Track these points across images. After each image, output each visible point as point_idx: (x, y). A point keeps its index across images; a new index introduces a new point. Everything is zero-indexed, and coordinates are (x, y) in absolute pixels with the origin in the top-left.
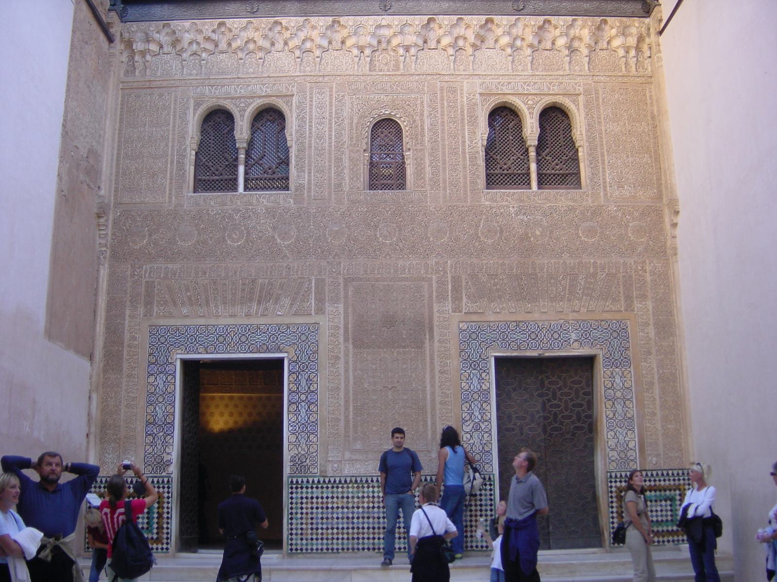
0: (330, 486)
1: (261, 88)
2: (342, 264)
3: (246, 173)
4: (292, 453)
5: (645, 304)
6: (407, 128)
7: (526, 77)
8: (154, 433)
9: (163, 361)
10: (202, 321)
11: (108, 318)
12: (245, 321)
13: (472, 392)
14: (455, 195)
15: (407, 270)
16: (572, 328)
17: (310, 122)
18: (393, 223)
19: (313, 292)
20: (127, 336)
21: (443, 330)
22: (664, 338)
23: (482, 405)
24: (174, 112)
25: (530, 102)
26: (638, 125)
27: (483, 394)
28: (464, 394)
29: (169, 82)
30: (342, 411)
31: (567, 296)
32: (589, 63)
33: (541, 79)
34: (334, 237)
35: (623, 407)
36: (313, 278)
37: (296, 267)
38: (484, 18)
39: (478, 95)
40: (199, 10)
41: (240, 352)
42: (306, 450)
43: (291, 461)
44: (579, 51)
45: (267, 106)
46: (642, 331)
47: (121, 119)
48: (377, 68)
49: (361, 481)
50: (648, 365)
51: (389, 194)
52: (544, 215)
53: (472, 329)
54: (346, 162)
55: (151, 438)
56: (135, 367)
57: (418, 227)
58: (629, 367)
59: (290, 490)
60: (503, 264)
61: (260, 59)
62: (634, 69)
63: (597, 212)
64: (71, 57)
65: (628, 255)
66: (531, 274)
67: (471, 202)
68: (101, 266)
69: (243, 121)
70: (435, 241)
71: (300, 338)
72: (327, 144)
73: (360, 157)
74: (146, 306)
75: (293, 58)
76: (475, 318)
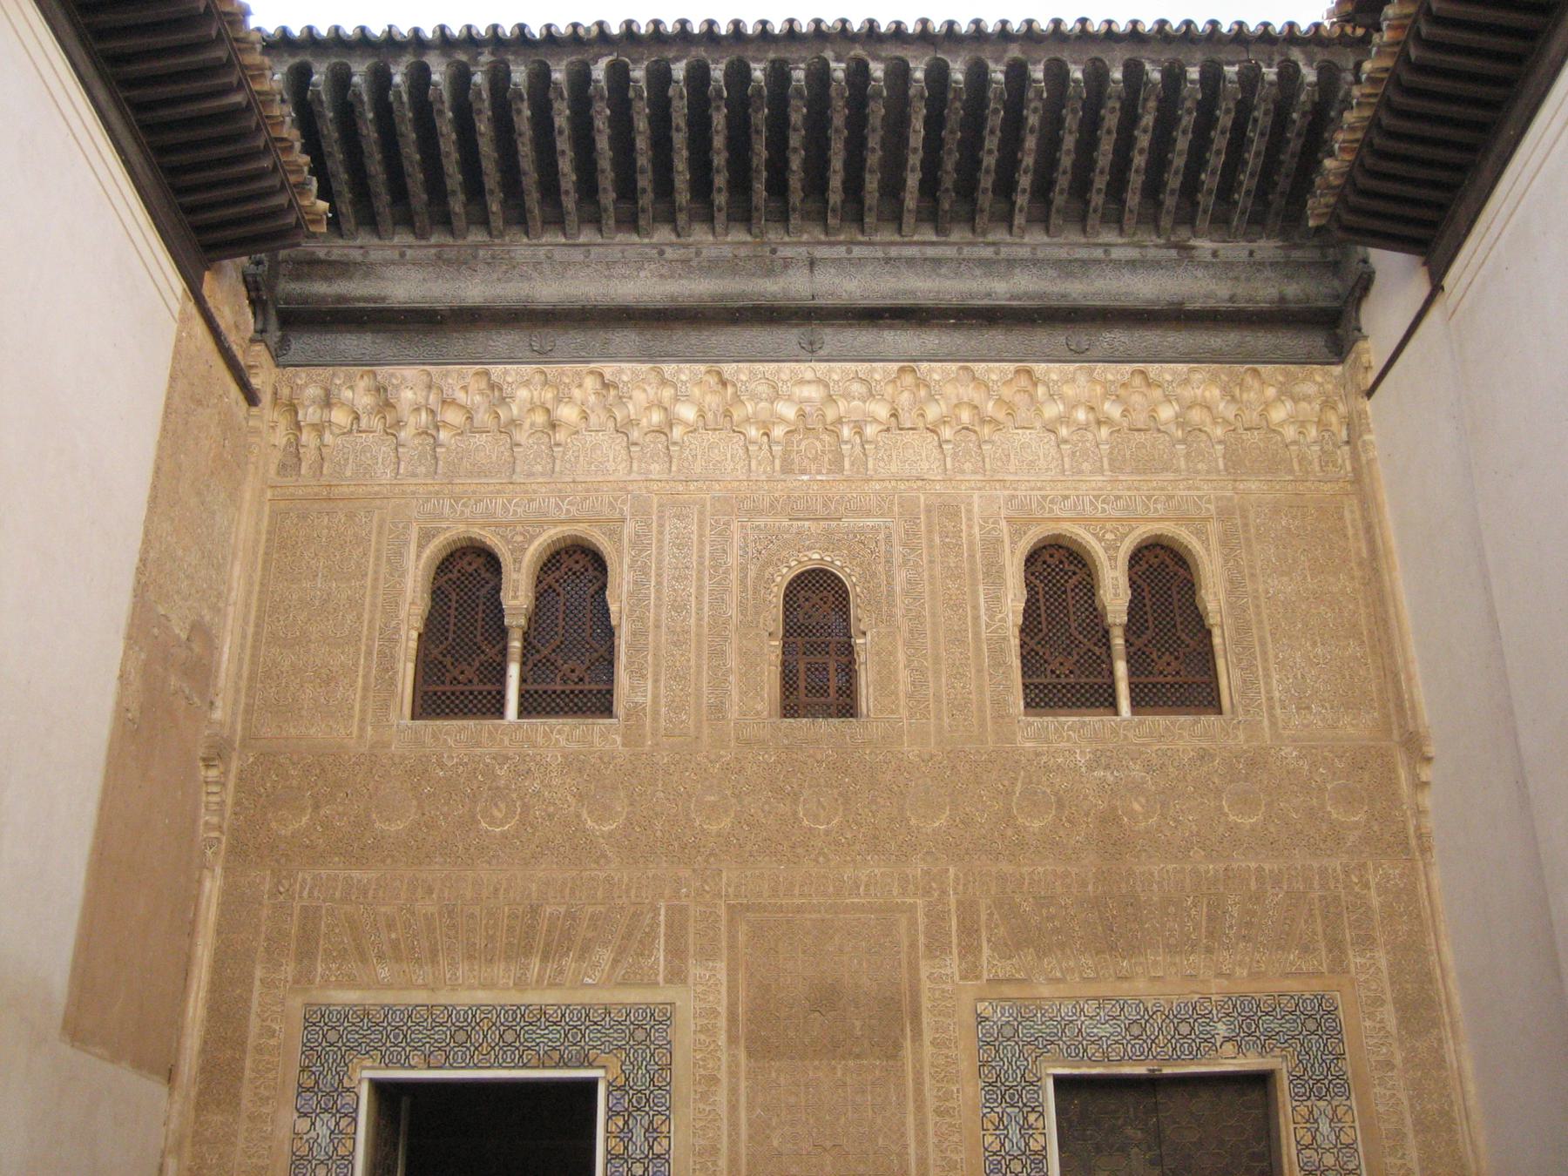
1: (557, 505)
2: (724, 874)
3: (523, 680)
5: (1372, 958)
7: (1099, 484)
9: (332, 1085)
10: (421, 997)
11: (215, 987)
12: (514, 998)
13: (1008, 1158)
14: (961, 728)
16: (1218, 1012)
20: (254, 1025)
24: (378, 550)
25: (1109, 536)
26: (1332, 579)
27: (1032, 1162)
28: (991, 1162)
33: (1129, 489)
36: (662, 905)
37: (626, 879)
39: (1003, 523)
40: (436, 346)
41: (501, 1067)
46: (1371, 1016)
47: (265, 562)
48: (796, 467)
50: (1388, 1093)
51: (827, 726)
52: (1148, 767)
54: (733, 662)
56: (268, 1098)
58: (1348, 1098)
60: (1066, 875)
62: (1318, 469)
64: (164, 429)
65: (1328, 852)
68: (206, 871)
69: (519, 571)
71: (631, 1034)
72: (693, 621)
73: (762, 648)
75: (624, 444)
76: (1009, 991)
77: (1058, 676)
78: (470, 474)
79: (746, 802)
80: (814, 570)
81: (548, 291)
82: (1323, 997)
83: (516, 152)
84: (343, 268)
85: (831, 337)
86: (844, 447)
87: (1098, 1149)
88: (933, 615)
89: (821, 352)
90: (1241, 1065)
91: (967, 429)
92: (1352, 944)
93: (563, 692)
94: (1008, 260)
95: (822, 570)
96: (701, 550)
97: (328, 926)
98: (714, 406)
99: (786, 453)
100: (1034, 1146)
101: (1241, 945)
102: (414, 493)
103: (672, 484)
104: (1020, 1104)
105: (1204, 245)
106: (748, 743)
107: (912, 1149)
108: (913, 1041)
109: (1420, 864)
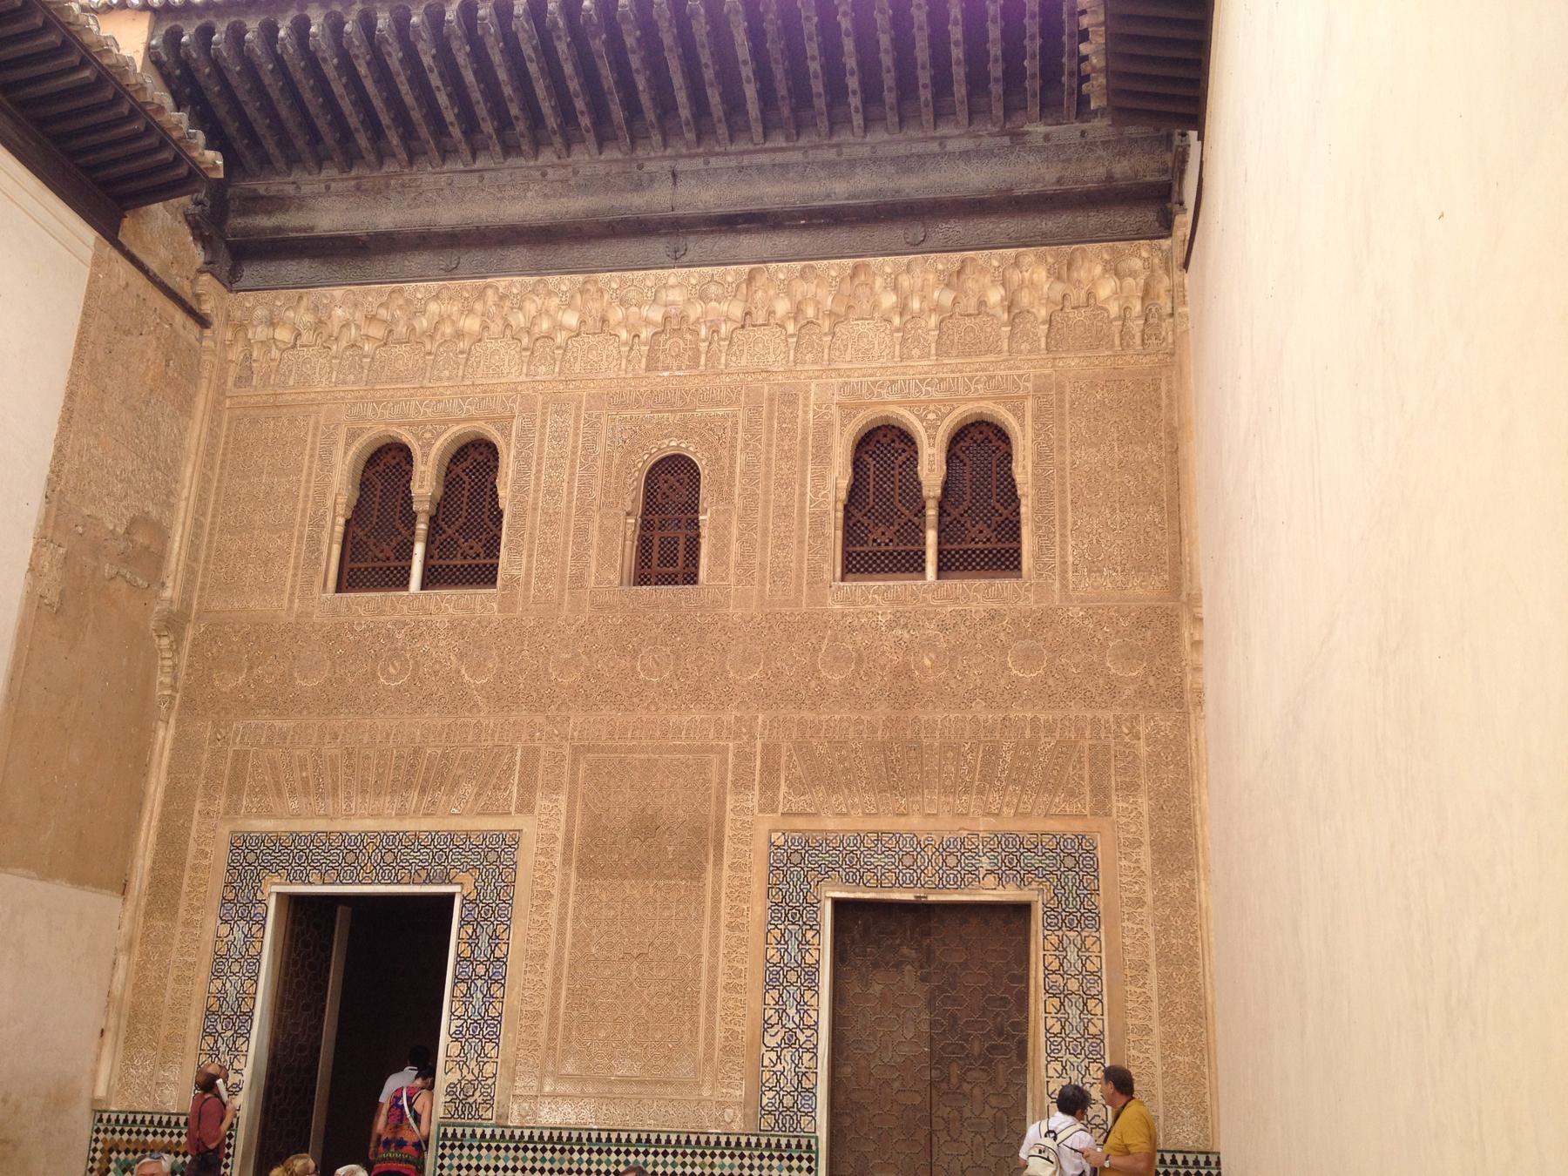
0: (512, 1145)
1: (459, 405)
2: (571, 721)
3: (428, 555)
4: (454, 1077)
5: (1135, 802)
6: (706, 472)
7: (926, 369)
8: (217, 1031)
10: (321, 825)
11: (164, 818)
12: (394, 825)
14: (780, 593)
15: (684, 732)
17: (539, 464)
19: (517, 772)
20: (192, 847)
21: (741, 846)
22: (1172, 873)
23: (802, 996)
25: (931, 416)
28: (771, 972)
29: (307, 396)
30: (547, 1001)
31: (977, 783)
32: (1047, 337)
33: (953, 372)
34: (562, 672)
35: (1082, 1012)
36: (519, 746)
37: (492, 725)
38: (850, 262)
39: (834, 409)
42: (476, 1071)
43: (448, 1094)
44: (1032, 313)
45: (473, 437)
46: (1126, 856)
47: (223, 461)
48: (660, 364)
49: (570, 1138)
50: (1136, 927)
52: (943, 628)
53: (793, 844)
54: (595, 536)
55: (210, 1040)
57: (710, 652)
58: (1098, 930)
59: (440, 1151)
60: (859, 722)
61: (462, 352)
62: (1138, 341)
63: (1043, 621)
66: (911, 741)
67: (808, 605)
68: (160, 723)
72: (563, 504)
74: (229, 796)
75: (518, 349)
76: (800, 823)
77: (879, 545)
78: (391, 380)
80: (674, 456)
81: (448, 215)
82: (1083, 837)
83: (399, 92)
84: (279, 203)
85: (696, 245)
87: (876, 966)
88: (766, 493)
89: (684, 259)
90: (1001, 896)
92: (1117, 790)
93: (462, 566)
94: (848, 160)
95: (680, 456)
97: (253, 766)
100: (809, 960)
101: (1010, 788)
102: (343, 398)
103: (554, 384)
104: (801, 923)
105: (1038, 129)
106: (601, 607)
107: (704, 959)
108: (715, 864)
109: (1192, 717)
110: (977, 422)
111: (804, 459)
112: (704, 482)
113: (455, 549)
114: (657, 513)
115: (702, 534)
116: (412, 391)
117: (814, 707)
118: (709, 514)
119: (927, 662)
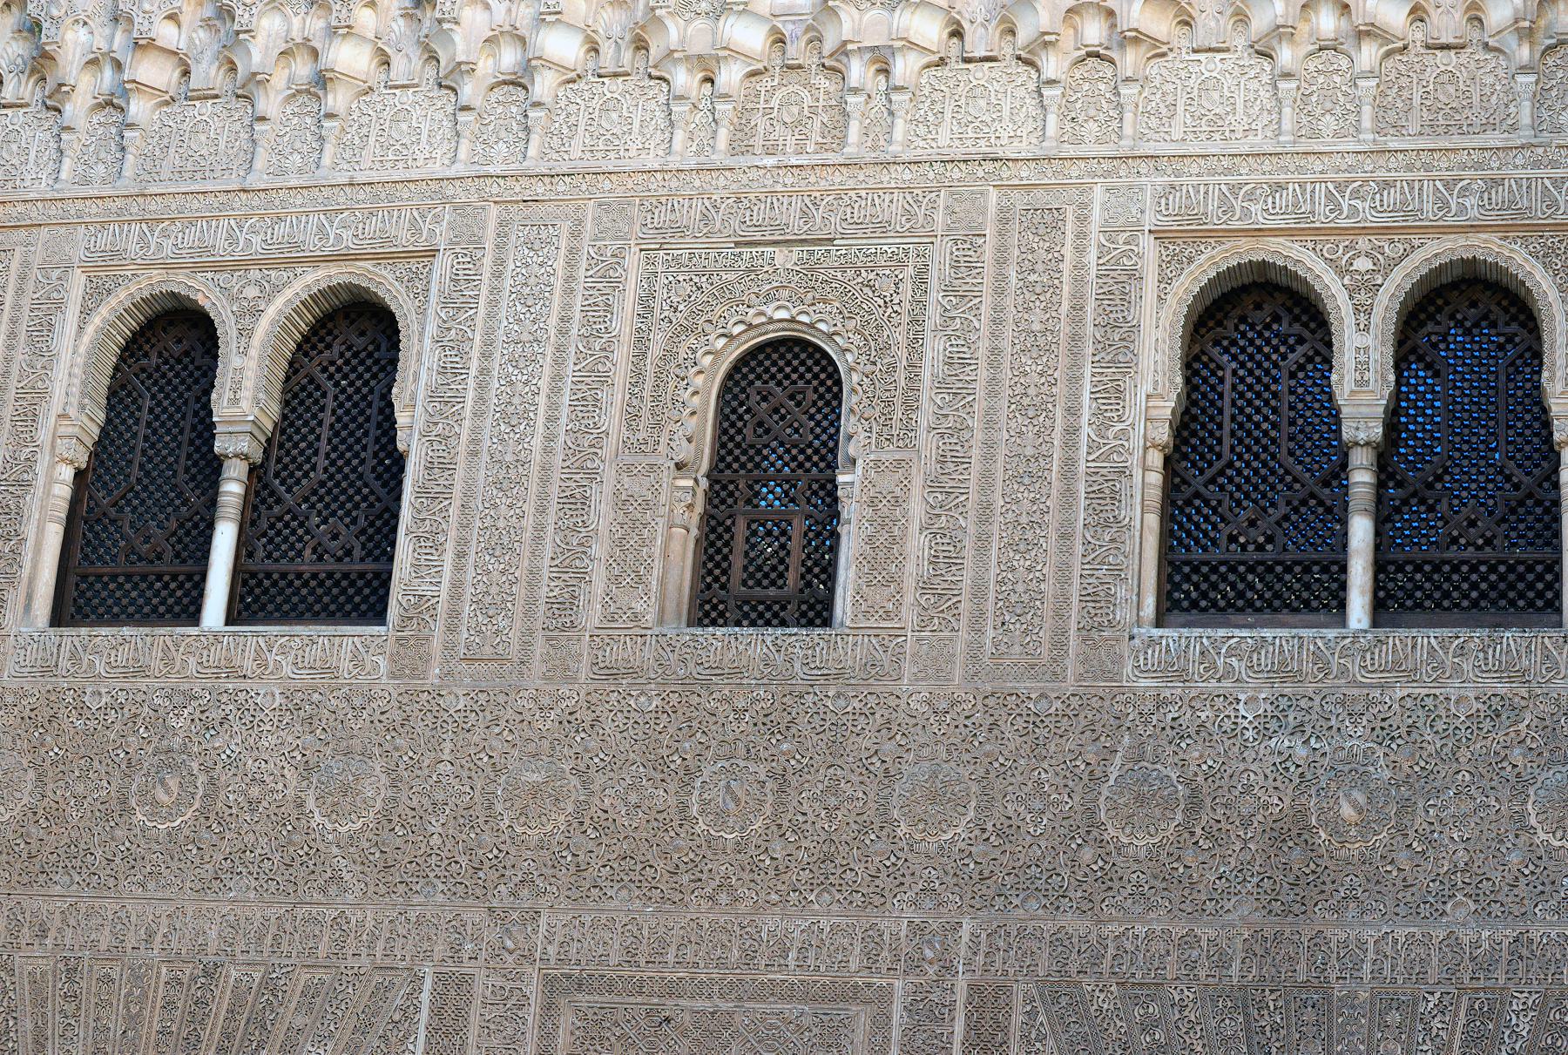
1: (321, 227)
2: (543, 921)
6: (855, 378)
7: (1350, 159)
14: (1017, 649)
15: (792, 955)
18: (757, 760)
25: (1363, 264)
33: (1410, 168)
36: (428, 971)
37: (370, 924)
39: (1148, 244)
45: (345, 296)
48: (758, 142)
52: (1384, 734)
54: (602, 514)
57: (855, 778)
66: (1305, 986)
67: (1080, 678)
70: (918, 837)
72: (537, 442)
75: (450, 109)
77: (1244, 547)
79: (596, 787)
86: (851, 99)
88: (990, 424)
91: (1098, 55)
93: (314, 576)
96: (567, 307)
98: (616, 31)
99: (744, 112)
103: (524, 182)
106: (612, 674)
110: (1463, 280)
111: (1075, 353)
112: (849, 401)
113: (300, 539)
114: (743, 466)
115: (844, 515)
116: (222, 198)
117: (1088, 906)
118: (859, 470)
119: (1347, 811)
